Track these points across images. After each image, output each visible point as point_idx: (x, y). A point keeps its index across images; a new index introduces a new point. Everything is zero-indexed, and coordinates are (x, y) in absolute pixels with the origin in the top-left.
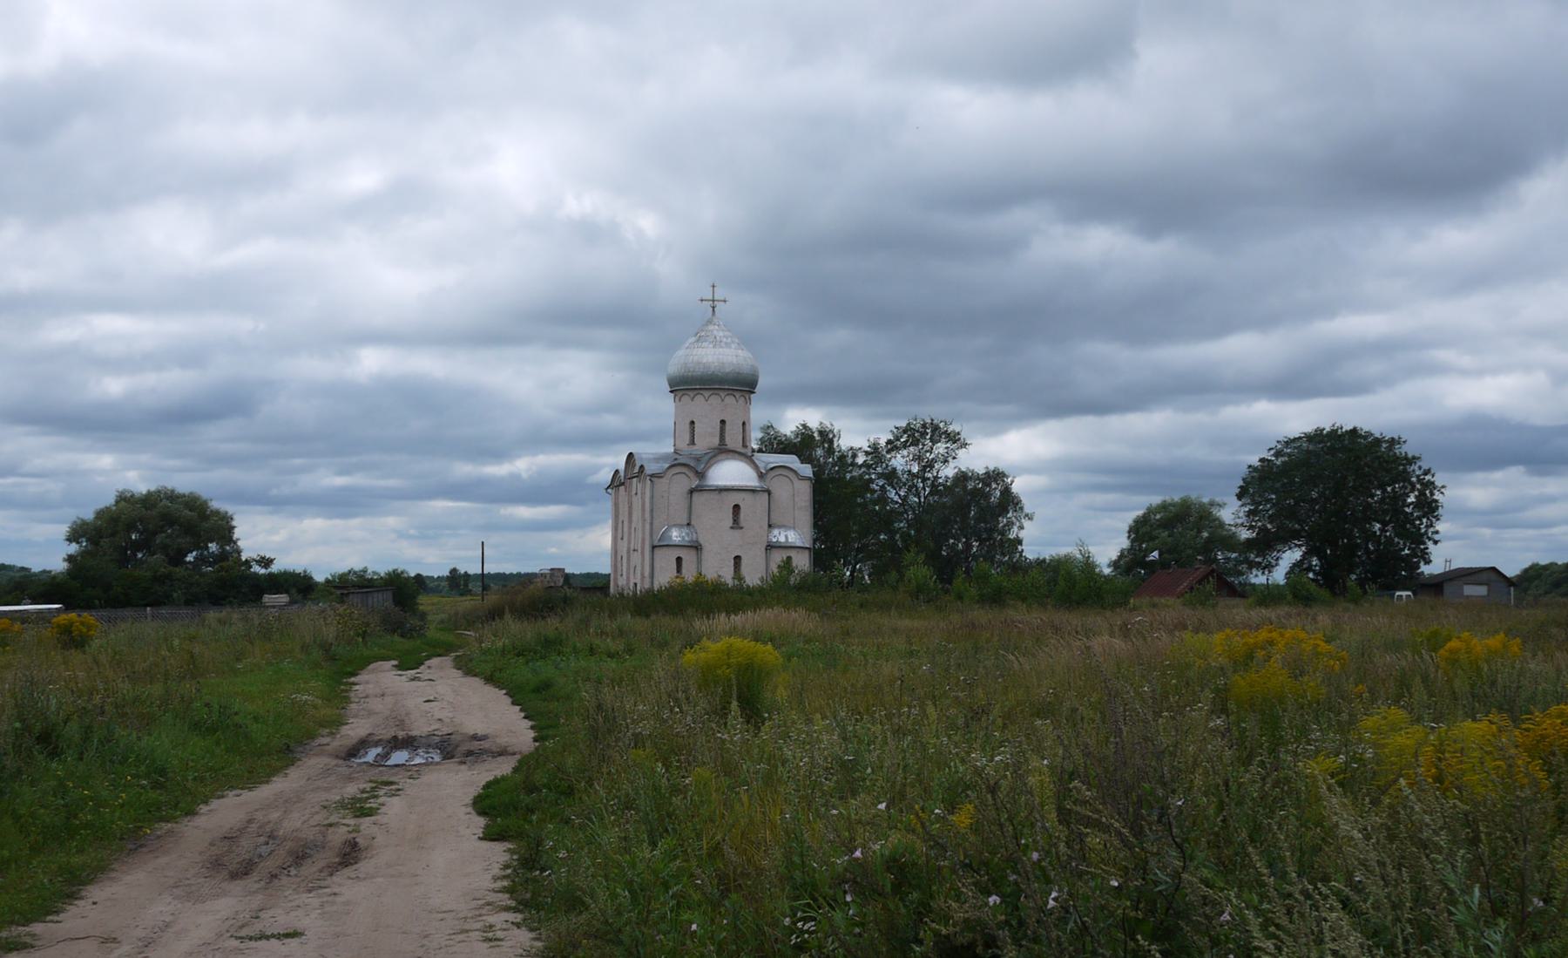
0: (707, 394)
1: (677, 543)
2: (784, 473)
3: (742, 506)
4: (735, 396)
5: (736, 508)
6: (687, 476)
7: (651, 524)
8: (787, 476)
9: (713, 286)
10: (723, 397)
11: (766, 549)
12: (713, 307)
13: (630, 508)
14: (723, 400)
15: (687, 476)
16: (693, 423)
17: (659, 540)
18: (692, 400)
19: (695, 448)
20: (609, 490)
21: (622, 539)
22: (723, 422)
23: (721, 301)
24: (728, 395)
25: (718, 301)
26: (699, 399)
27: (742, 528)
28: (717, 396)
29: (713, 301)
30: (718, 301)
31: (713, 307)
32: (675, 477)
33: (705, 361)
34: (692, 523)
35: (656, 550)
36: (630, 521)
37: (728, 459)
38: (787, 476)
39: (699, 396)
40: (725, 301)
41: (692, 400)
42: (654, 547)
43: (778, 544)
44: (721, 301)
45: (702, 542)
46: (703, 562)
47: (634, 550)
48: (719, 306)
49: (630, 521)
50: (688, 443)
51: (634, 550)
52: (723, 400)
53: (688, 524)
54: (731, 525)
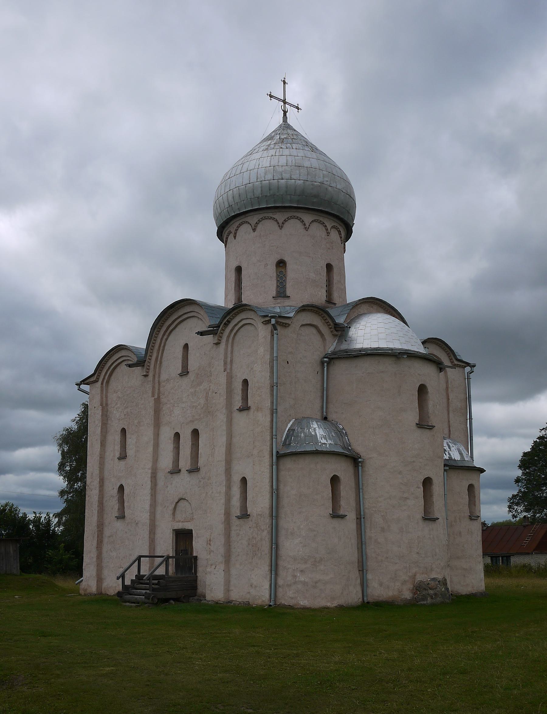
0: (308, 218)
1: (328, 448)
3: (430, 389)
4: (339, 232)
5: (422, 390)
6: (319, 331)
7: (273, 412)
10: (329, 227)
12: (285, 112)
13: (158, 401)
15: (319, 331)
16: (281, 264)
17: (286, 444)
18: (281, 227)
19: (287, 302)
20: (83, 387)
21: (123, 457)
22: (329, 267)
24: (333, 227)
25: (291, 105)
26: (294, 226)
27: (431, 428)
28: (321, 226)
29: (285, 102)
30: (291, 105)
31: (285, 112)
32: (302, 328)
33: (307, 164)
35: (288, 464)
36: (157, 424)
37: (370, 313)
39: (292, 221)
40: (298, 108)
41: (281, 227)
42: (280, 456)
45: (359, 447)
47: (176, 471)
48: (291, 112)
49: (157, 424)
50: (274, 293)
51: (176, 471)
52: (328, 234)
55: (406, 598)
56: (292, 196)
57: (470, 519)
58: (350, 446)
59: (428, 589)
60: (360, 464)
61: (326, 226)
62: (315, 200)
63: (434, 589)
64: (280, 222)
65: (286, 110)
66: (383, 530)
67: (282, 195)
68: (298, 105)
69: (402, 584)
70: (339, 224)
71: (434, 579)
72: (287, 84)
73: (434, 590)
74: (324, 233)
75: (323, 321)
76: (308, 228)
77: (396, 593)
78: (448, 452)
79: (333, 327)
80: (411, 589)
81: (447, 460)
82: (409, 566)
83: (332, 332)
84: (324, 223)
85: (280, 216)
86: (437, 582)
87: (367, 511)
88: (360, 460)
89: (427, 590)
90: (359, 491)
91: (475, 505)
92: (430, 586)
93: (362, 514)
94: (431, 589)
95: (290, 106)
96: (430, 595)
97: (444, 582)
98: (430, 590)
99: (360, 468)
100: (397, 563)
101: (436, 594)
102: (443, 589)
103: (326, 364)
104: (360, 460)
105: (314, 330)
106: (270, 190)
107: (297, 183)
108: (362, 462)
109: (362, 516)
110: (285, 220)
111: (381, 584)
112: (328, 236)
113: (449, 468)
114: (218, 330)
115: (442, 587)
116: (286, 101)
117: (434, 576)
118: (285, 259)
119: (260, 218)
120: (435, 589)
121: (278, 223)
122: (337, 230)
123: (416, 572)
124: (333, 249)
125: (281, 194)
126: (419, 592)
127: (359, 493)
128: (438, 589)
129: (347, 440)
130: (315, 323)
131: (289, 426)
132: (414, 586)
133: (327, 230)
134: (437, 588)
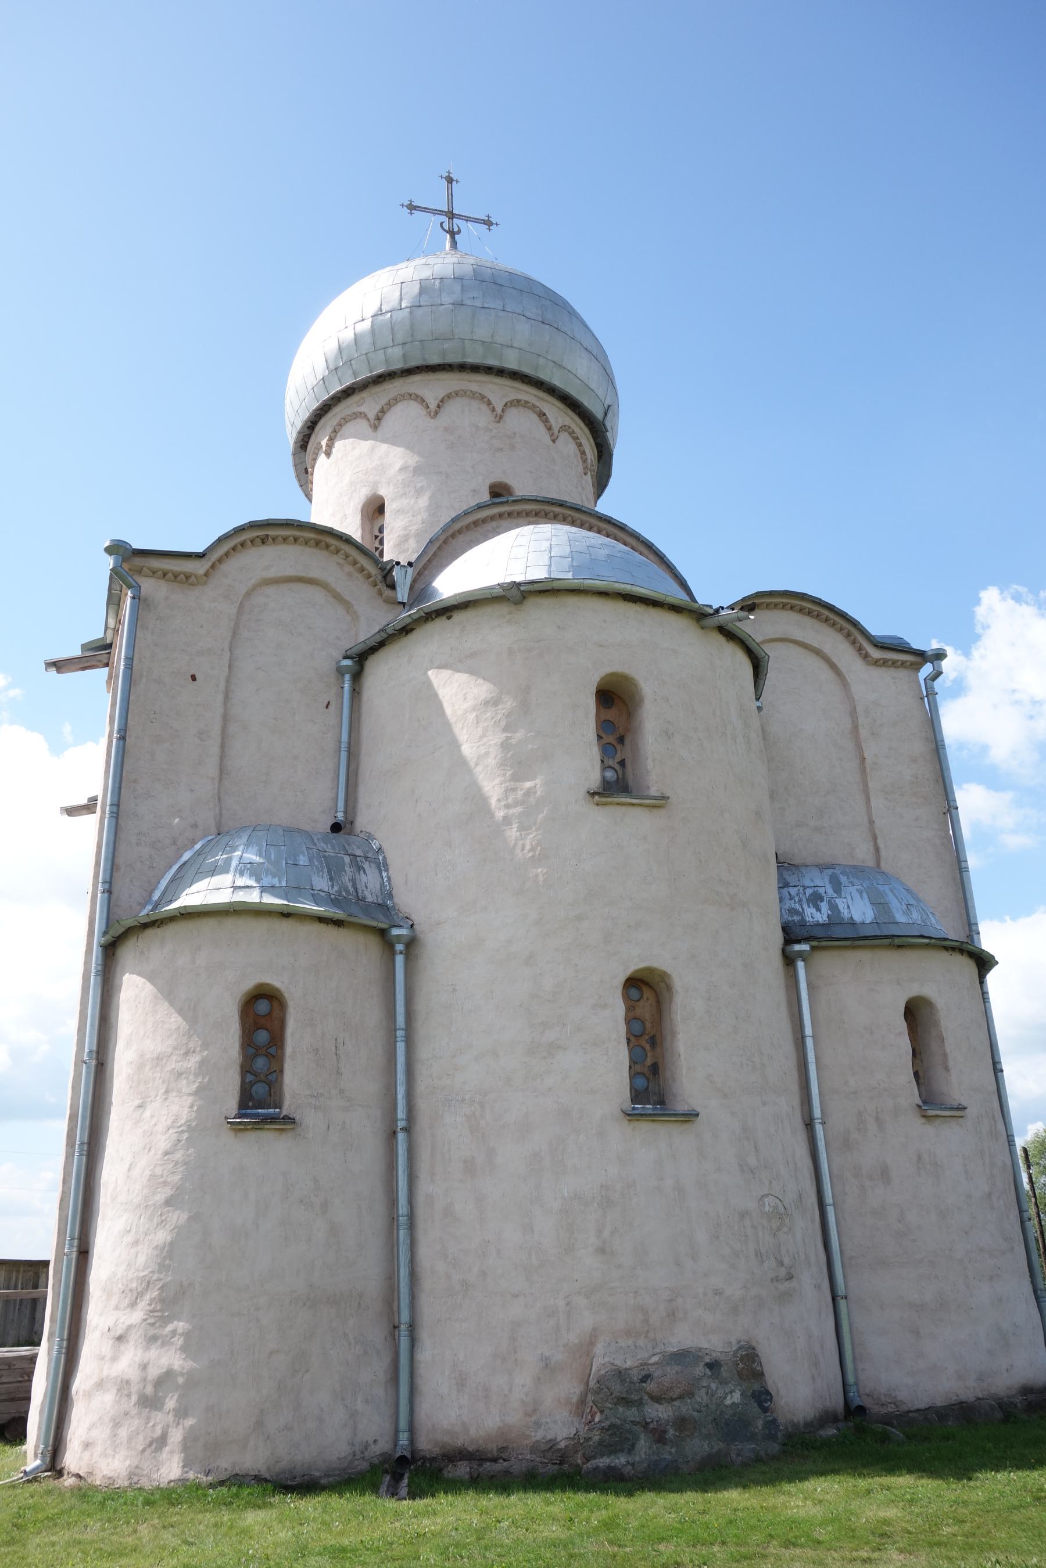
0: (433, 387)
2: (798, 635)
4: (542, 415)
6: (338, 597)
8: (817, 652)
9: (450, 180)
11: (789, 960)
14: (500, 418)
15: (338, 597)
23: (476, 220)
24: (517, 403)
25: (467, 219)
27: (660, 803)
28: (475, 404)
29: (451, 215)
30: (467, 219)
32: (270, 590)
34: (363, 822)
38: (817, 652)
40: (488, 223)
43: (838, 932)
44: (476, 220)
46: (422, 1029)
53: (336, 828)
54: (593, 777)
55: (550, 1440)
56: (390, 350)
57: (924, 1116)
58: (390, 896)
59: (646, 1397)
60: (399, 947)
61: (489, 403)
62: (446, 346)
63: (672, 1400)
64: (372, 415)
65: (456, 229)
66: (470, 1168)
67: (366, 354)
68: (488, 216)
69: (539, 1379)
70: (535, 396)
71: (681, 1357)
72: (457, 181)
73: (676, 1403)
74: (482, 417)
75: (348, 568)
76: (436, 413)
77: (515, 1418)
78: (829, 902)
79: (380, 577)
80: (575, 1400)
81: (823, 925)
82: (568, 1304)
83: (380, 593)
84: (482, 397)
85: (369, 403)
86: (700, 1370)
87: (423, 1106)
88: (395, 932)
89: (640, 1403)
90: (396, 1037)
91: (947, 1069)
92: (652, 1385)
93: (401, 1113)
94: (657, 1399)
95: (466, 220)
96: (651, 1426)
97: (741, 1365)
98: (657, 1405)
99: (400, 960)
100: (518, 1296)
101: (681, 1423)
102: (736, 1397)
103: (347, 677)
104: (395, 932)
105: (318, 595)
106: (341, 353)
107: (394, 318)
108: (412, 944)
109: (401, 1124)
110: (383, 411)
111: (461, 1383)
112: (499, 422)
113: (813, 948)
114: (110, 653)
115: (731, 1386)
116: (454, 212)
117: (682, 1337)
118: (382, 492)
119: (335, 423)
120: (681, 1397)
121: (368, 420)
122: (535, 412)
123: (594, 1329)
124: (512, 447)
125: (364, 352)
126: (602, 1412)
127: (395, 1042)
128: (701, 1397)
129: (385, 879)
130: (314, 573)
131: (187, 856)
132: (587, 1389)
133: (493, 410)
134: (691, 1394)
